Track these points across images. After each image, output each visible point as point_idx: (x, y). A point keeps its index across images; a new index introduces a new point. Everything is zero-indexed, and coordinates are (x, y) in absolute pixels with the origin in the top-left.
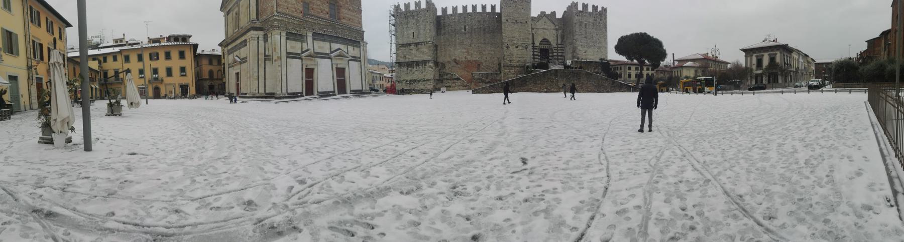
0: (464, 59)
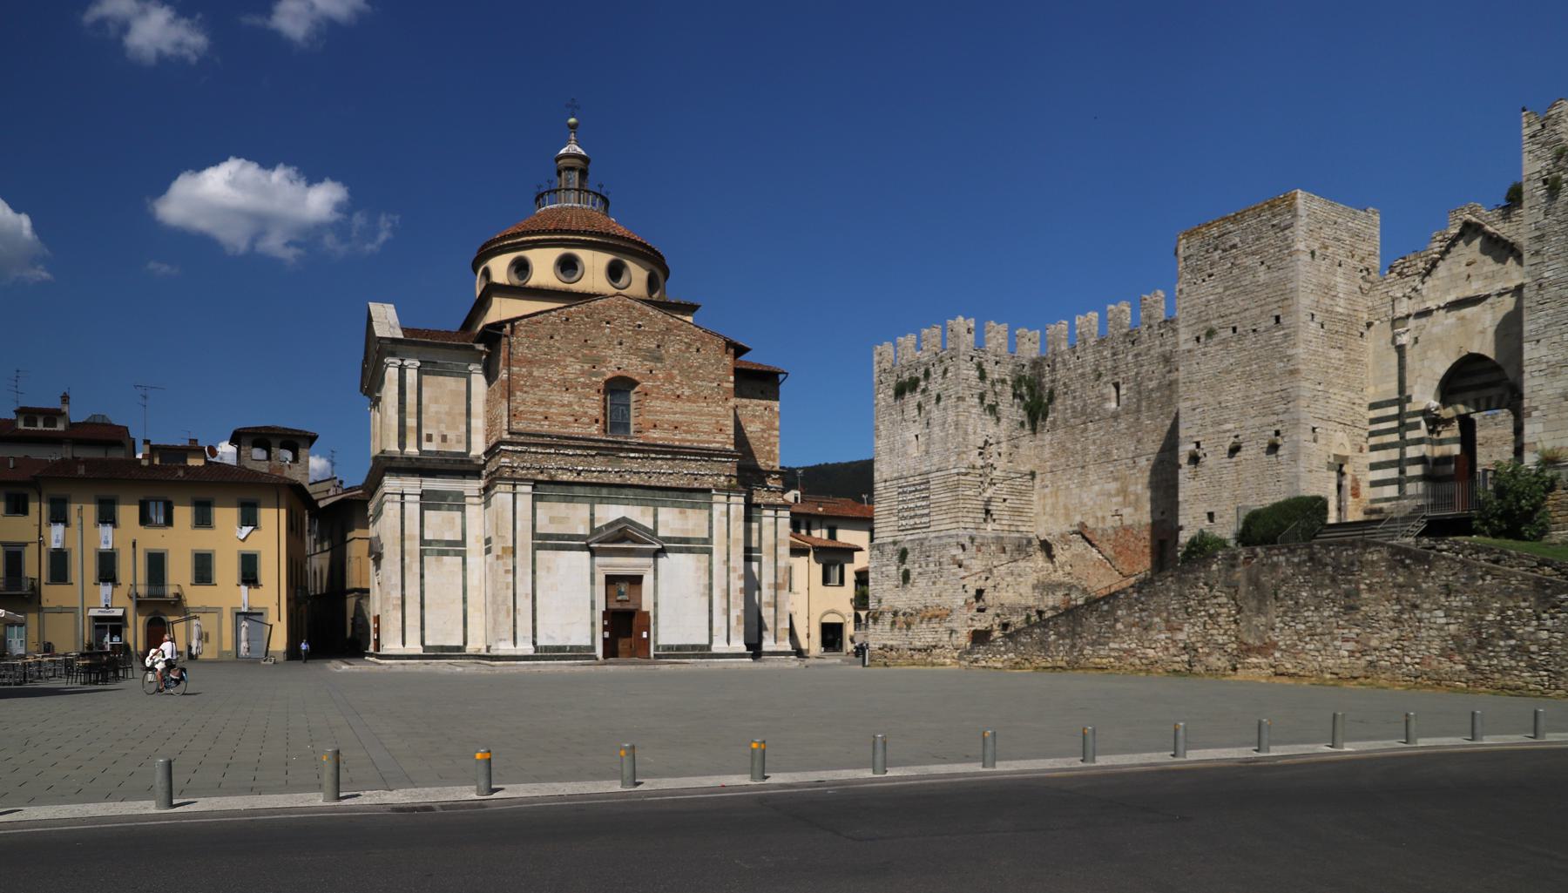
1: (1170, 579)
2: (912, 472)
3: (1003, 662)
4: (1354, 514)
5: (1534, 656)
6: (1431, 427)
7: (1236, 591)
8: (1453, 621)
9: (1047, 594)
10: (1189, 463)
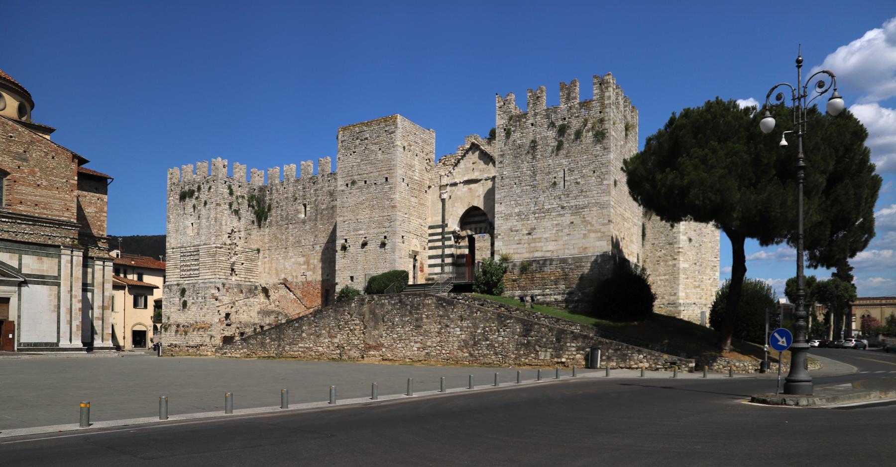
1: (331, 310)
2: (189, 244)
3: (240, 354)
4: (421, 281)
5: (497, 349)
6: (456, 240)
7: (364, 317)
8: (463, 333)
9: (266, 317)
10: (341, 250)
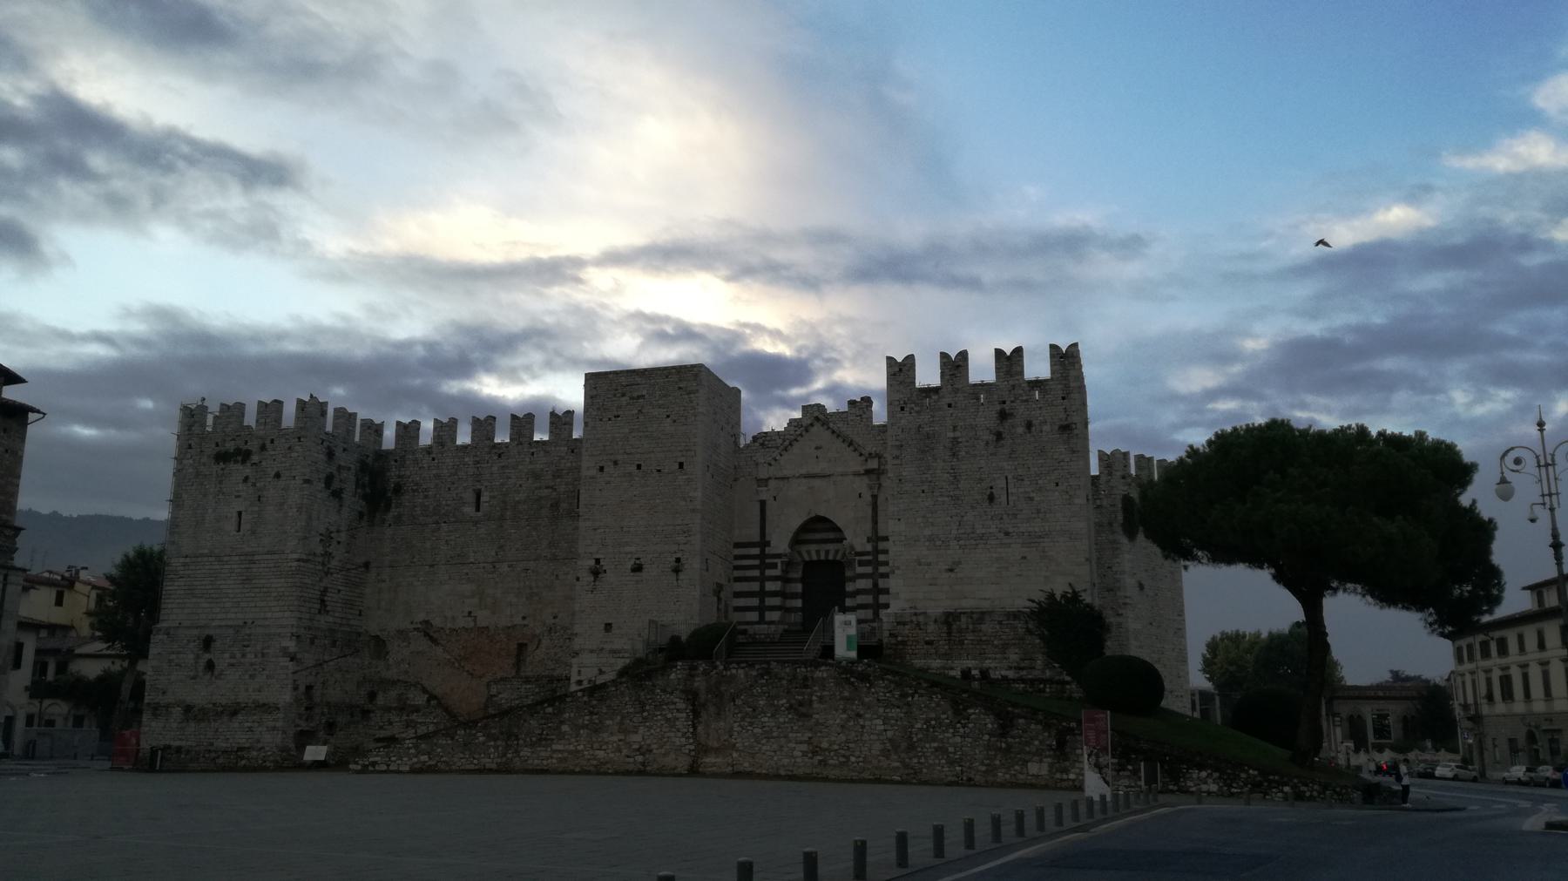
0: (462, 622)
8: (889, 728)
